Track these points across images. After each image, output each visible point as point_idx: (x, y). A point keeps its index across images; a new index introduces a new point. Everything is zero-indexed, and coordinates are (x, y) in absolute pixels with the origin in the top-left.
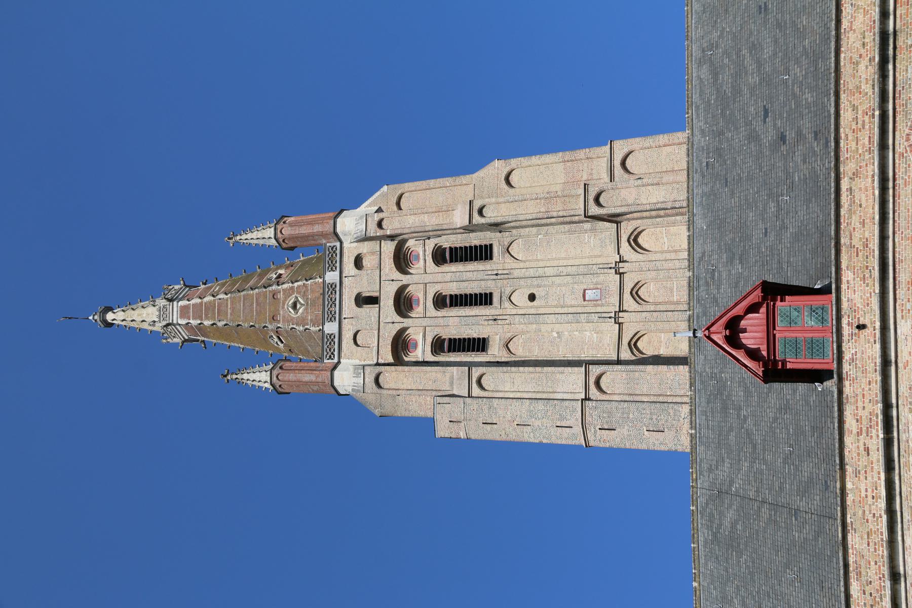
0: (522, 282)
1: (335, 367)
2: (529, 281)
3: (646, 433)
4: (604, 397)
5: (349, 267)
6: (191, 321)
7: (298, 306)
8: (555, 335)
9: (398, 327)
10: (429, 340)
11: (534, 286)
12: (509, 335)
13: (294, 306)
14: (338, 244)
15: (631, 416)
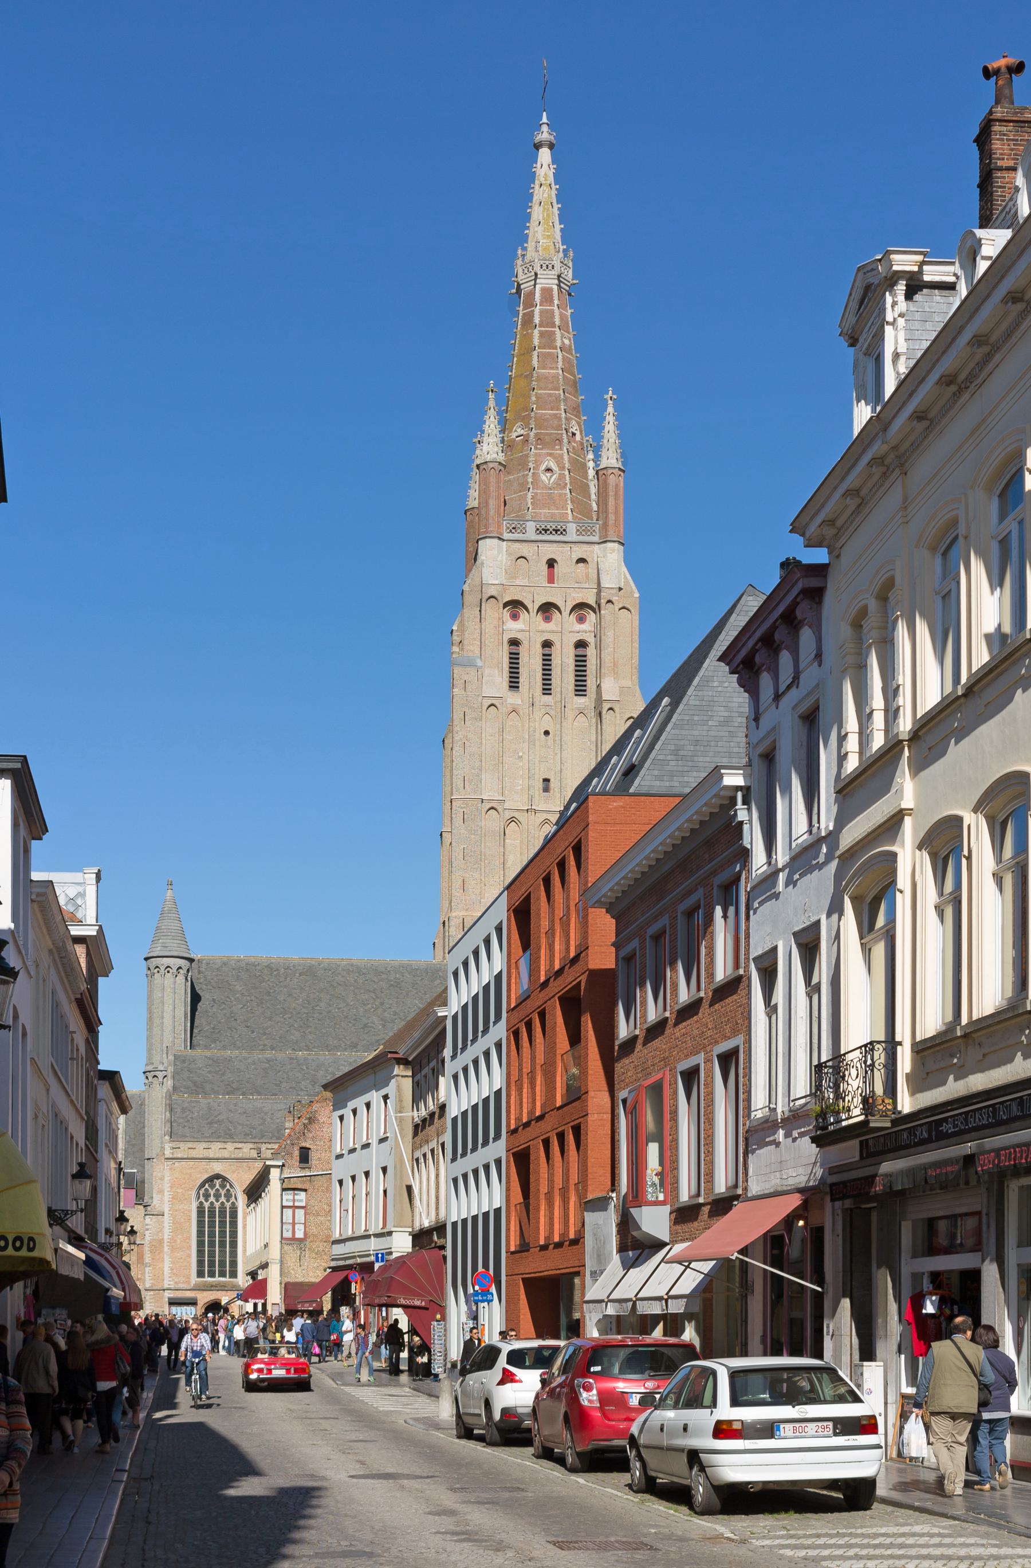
0: (558, 726)
1: (500, 539)
2: (558, 733)
3: (462, 847)
4: (483, 814)
5: (579, 552)
6: (538, 307)
7: (548, 475)
8: (521, 754)
9: (530, 606)
10: (519, 636)
11: (555, 736)
12: (521, 713)
13: (548, 470)
14: (596, 539)
15: (473, 836)
